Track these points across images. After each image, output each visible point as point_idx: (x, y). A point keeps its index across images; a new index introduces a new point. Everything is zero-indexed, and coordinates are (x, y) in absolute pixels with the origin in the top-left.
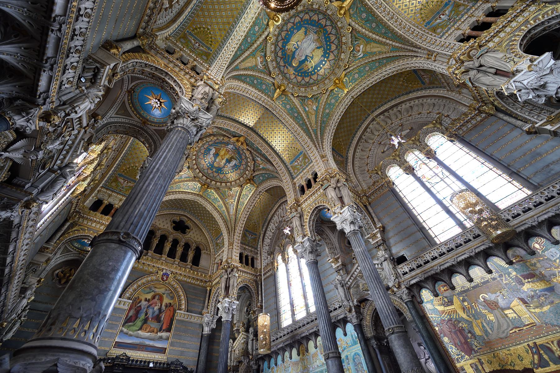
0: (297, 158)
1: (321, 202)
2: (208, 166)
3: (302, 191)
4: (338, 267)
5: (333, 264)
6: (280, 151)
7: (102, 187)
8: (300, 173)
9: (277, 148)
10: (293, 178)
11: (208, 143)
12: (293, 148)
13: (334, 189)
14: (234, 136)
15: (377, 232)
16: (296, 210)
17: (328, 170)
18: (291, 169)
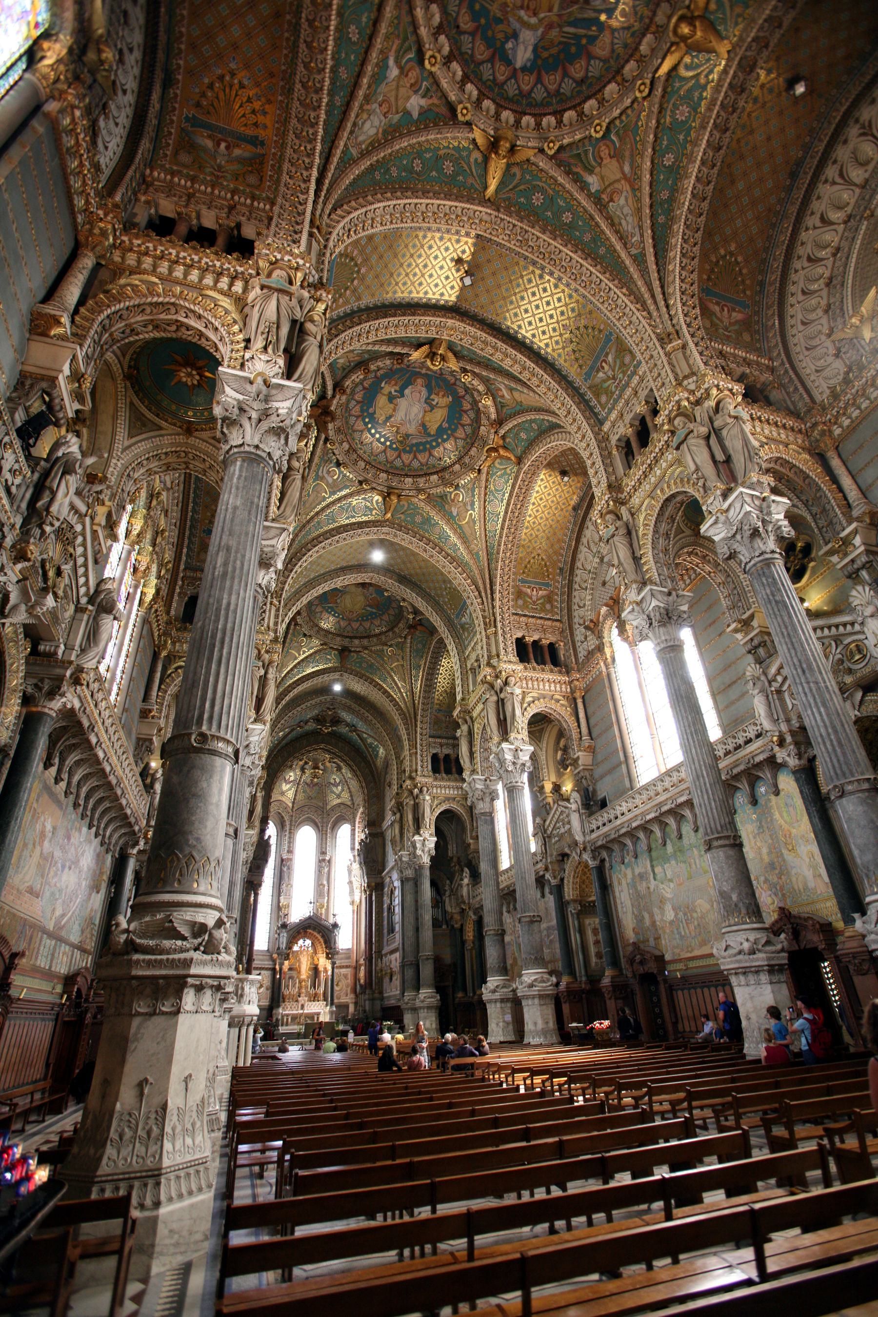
0: (598, 357)
1: (675, 483)
2: (383, 444)
3: (628, 453)
4: (752, 639)
5: (739, 636)
6: (549, 350)
7: (185, 569)
8: (616, 401)
9: (540, 343)
10: (599, 420)
11: (361, 387)
12: (582, 329)
13: (702, 442)
14: (419, 346)
15: (855, 532)
16: (617, 516)
17: (685, 383)
18: (589, 395)
